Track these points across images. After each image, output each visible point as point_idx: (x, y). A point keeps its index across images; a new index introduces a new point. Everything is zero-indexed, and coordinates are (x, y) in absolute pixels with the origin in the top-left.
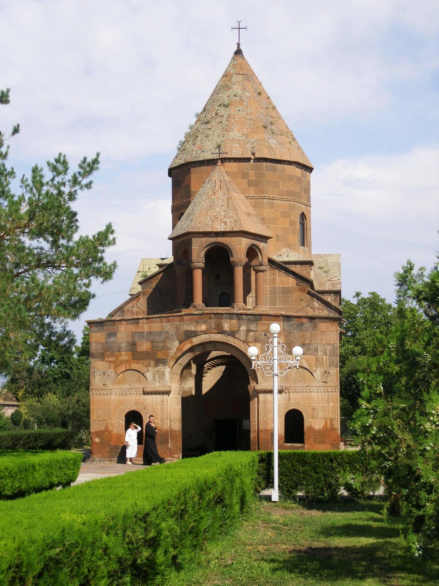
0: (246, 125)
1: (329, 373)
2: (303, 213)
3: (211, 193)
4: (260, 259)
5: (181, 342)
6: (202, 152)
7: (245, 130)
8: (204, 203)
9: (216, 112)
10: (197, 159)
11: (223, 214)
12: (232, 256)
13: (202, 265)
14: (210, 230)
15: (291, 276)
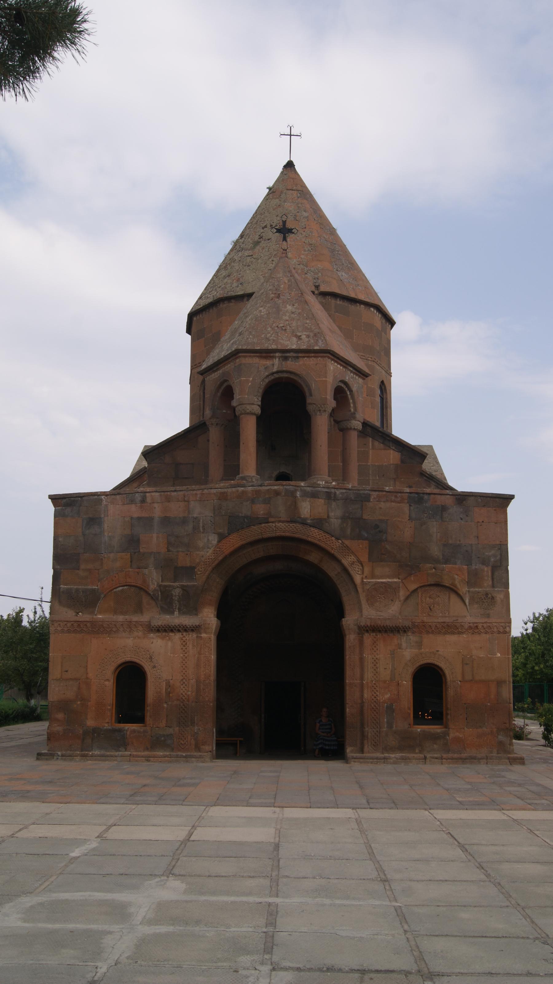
0: (305, 251)
1: (493, 598)
2: (382, 382)
3: (273, 295)
4: (352, 410)
5: (222, 537)
6: (241, 284)
7: (302, 256)
8: (261, 309)
9: (259, 236)
10: (233, 294)
11: (294, 324)
12: (311, 395)
13: (257, 410)
14: (274, 347)
15: (393, 448)
